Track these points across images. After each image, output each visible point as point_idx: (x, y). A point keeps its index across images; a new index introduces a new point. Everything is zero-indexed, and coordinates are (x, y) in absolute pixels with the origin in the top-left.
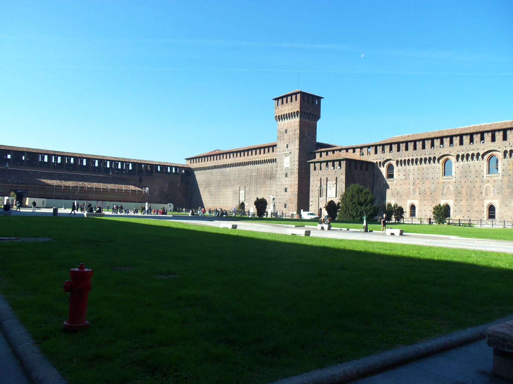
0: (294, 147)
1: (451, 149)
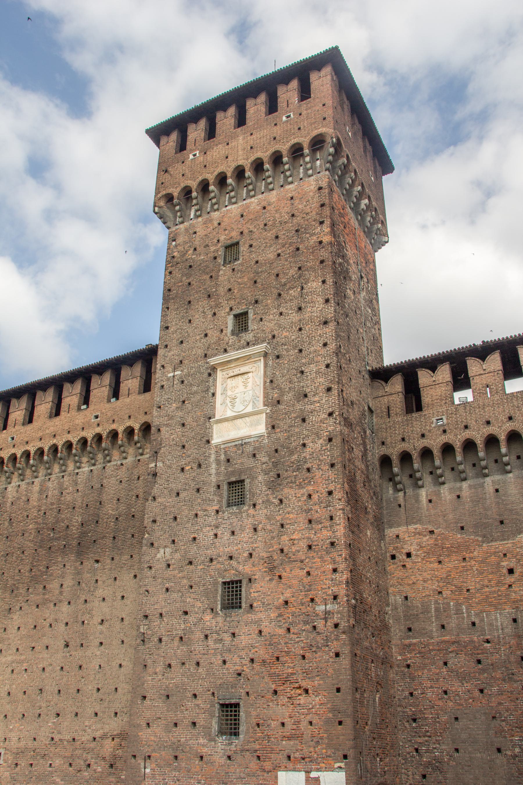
0: (295, 317)
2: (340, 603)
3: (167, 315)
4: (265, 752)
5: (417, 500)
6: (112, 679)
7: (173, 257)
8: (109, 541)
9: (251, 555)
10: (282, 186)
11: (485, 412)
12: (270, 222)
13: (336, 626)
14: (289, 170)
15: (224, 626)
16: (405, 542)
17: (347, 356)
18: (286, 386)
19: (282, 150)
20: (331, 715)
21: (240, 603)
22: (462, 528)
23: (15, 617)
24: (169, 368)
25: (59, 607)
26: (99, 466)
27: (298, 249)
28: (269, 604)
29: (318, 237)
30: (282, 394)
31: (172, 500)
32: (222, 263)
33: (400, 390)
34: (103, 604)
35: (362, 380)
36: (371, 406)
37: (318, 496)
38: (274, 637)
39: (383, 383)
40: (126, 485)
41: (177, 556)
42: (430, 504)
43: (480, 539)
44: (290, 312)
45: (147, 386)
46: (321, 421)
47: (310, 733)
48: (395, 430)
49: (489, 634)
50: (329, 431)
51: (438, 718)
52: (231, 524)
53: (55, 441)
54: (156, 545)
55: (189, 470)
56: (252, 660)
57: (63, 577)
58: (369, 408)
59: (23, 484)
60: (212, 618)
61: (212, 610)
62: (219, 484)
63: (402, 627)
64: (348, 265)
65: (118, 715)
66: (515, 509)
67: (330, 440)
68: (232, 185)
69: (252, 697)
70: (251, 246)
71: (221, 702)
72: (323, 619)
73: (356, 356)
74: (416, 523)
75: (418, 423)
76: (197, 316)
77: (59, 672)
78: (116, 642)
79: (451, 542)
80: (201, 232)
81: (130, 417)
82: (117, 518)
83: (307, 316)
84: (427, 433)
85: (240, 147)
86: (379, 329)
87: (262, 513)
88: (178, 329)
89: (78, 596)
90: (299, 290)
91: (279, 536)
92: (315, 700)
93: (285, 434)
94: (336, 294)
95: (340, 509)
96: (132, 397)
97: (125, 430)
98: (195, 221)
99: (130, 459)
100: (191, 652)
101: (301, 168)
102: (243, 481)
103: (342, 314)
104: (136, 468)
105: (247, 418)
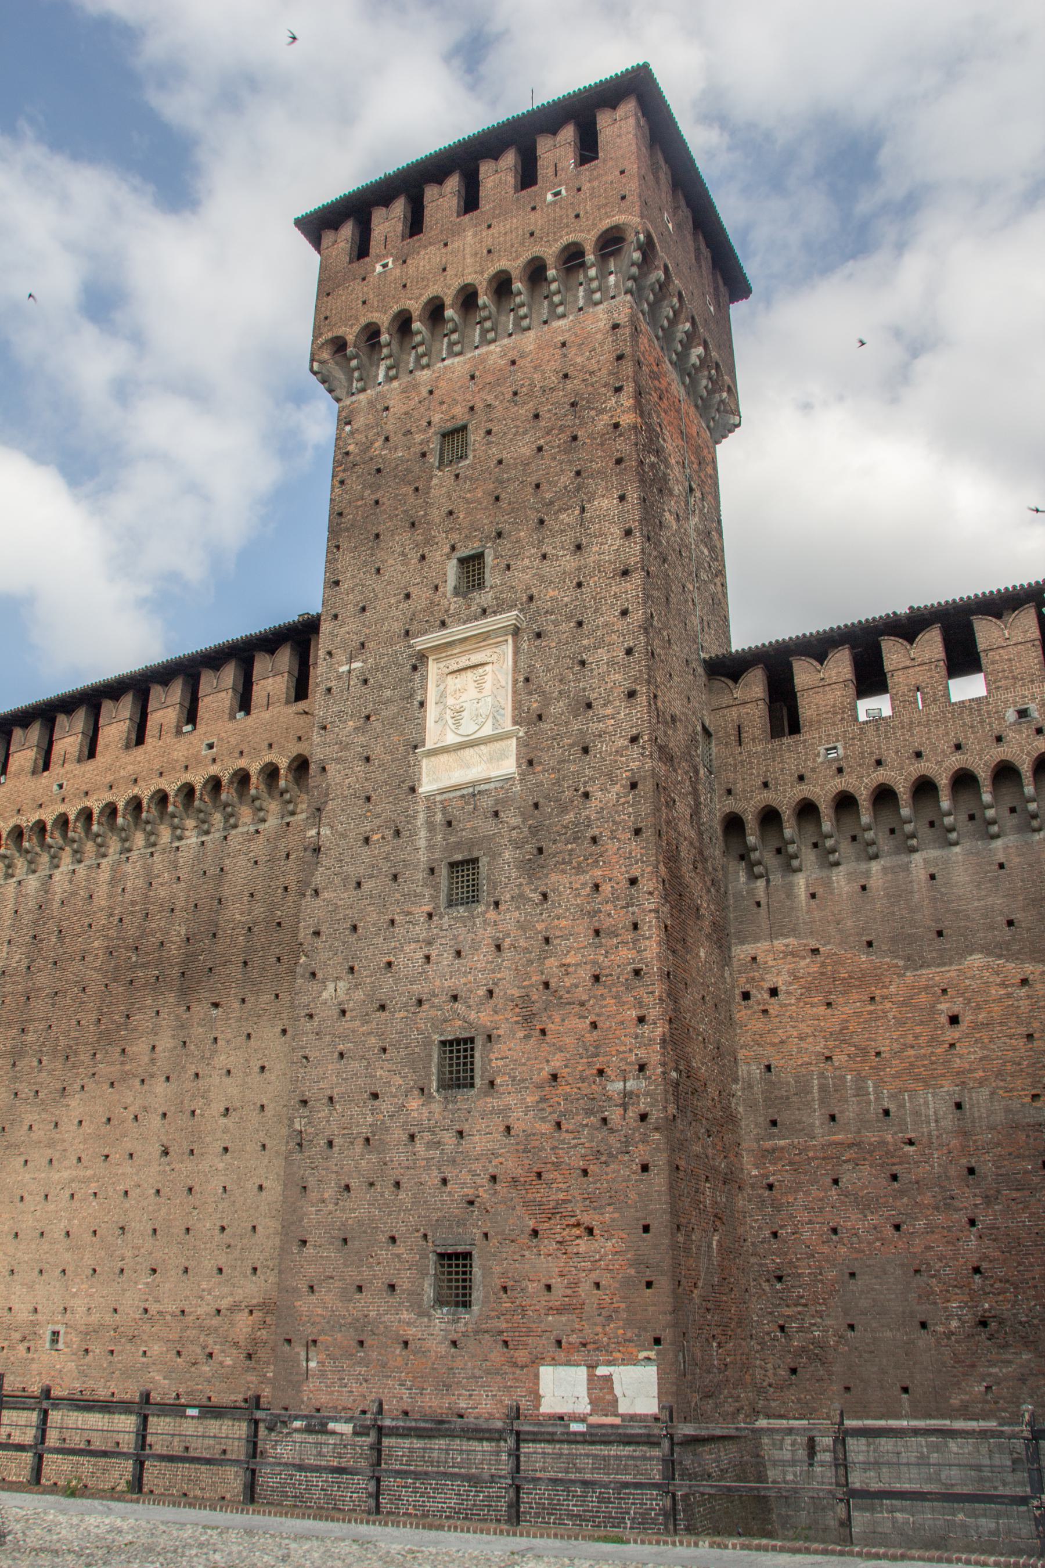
0: (569, 562)
2: (650, 1078)
3: (336, 560)
4: (517, 1334)
5: (790, 894)
6: (247, 1211)
7: (347, 453)
8: (235, 970)
9: (490, 992)
10: (545, 322)
11: (912, 735)
12: (524, 389)
13: (643, 1117)
14: (559, 292)
15: (444, 1118)
16: (767, 969)
17: (665, 633)
18: (553, 688)
19: (545, 256)
20: (632, 1272)
21: (472, 1078)
22: (870, 944)
23: (73, 1103)
24: (341, 656)
25: (150, 1085)
26: (216, 835)
27: (575, 438)
28: (523, 1080)
29: (612, 416)
30: (547, 702)
31: (348, 895)
32: (437, 464)
33: (760, 695)
34: (227, 1081)
35: (691, 677)
36: (707, 724)
37: (612, 887)
38: (532, 1137)
39: (730, 683)
40: (266, 869)
41: (359, 995)
42: (812, 902)
43: (901, 963)
44: (561, 553)
45: (301, 690)
46: (617, 751)
47: (597, 1301)
48: (751, 768)
49: (914, 1131)
50: (632, 770)
51: (821, 1274)
52: (455, 937)
53: (136, 791)
54: (320, 975)
55: (378, 840)
56: (494, 1178)
57: (156, 1034)
58: (705, 729)
59: (81, 869)
60: (423, 1105)
61: (422, 1090)
62: (433, 865)
63: (761, 1119)
64: (667, 467)
65: (258, 1272)
66: (964, 910)
67: (634, 786)
68: (453, 320)
69: (494, 1241)
70: (489, 432)
71: (439, 1251)
72: (620, 1105)
73: (681, 633)
74: (787, 936)
75: (791, 755)
76: (391, 562)
77: (153, 1199)
78: (253, 1147)
79: (850, 968)
80: (397, 406)
81: (270, 746)
82: (250, 928)
83: (591, 560)
84: (808, 775)
85: (468, 250)
86: (722, 585)
87: (510, 917)
88: (357, 585)
89: (183, 1067)
90: (577, 512)
91: (542, 959)
92: (604, 1246)
93: (553, 776)
94: (644, 520)
95: (650, 911)
96: (274, 710)
97: (262, 769)
98: (386, 387)
99: (273, 822)
100: (385, 1164)
101: (581, 289)
102: (475, 861)
103: (656, 557)
104: (283, 837)
105: (483, 747)
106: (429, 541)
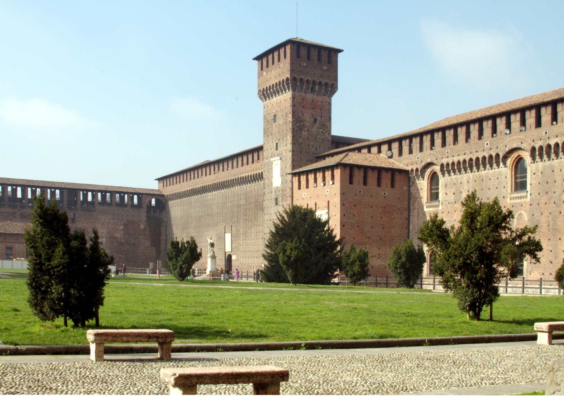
0: (285, 148)
1: (522, 136)
106: (273, 139)
